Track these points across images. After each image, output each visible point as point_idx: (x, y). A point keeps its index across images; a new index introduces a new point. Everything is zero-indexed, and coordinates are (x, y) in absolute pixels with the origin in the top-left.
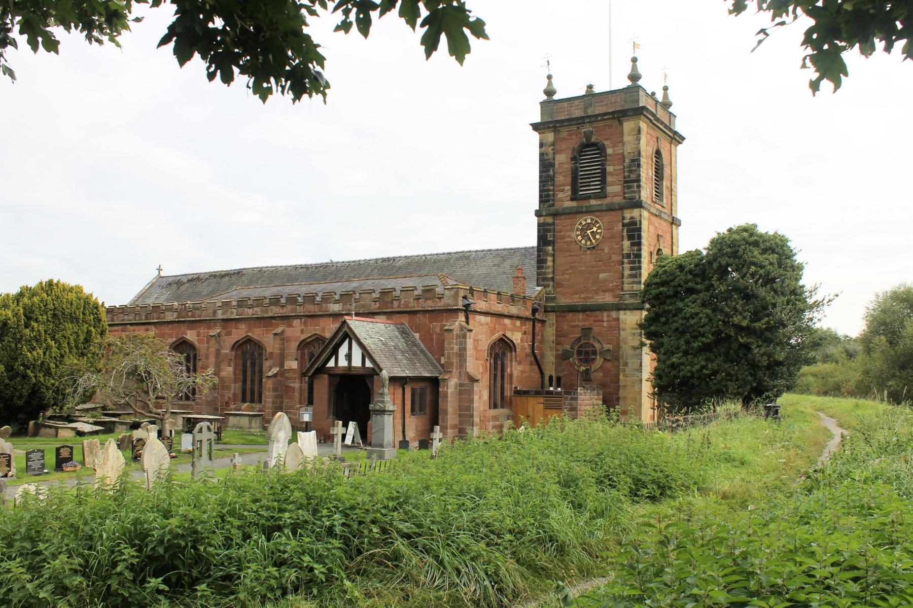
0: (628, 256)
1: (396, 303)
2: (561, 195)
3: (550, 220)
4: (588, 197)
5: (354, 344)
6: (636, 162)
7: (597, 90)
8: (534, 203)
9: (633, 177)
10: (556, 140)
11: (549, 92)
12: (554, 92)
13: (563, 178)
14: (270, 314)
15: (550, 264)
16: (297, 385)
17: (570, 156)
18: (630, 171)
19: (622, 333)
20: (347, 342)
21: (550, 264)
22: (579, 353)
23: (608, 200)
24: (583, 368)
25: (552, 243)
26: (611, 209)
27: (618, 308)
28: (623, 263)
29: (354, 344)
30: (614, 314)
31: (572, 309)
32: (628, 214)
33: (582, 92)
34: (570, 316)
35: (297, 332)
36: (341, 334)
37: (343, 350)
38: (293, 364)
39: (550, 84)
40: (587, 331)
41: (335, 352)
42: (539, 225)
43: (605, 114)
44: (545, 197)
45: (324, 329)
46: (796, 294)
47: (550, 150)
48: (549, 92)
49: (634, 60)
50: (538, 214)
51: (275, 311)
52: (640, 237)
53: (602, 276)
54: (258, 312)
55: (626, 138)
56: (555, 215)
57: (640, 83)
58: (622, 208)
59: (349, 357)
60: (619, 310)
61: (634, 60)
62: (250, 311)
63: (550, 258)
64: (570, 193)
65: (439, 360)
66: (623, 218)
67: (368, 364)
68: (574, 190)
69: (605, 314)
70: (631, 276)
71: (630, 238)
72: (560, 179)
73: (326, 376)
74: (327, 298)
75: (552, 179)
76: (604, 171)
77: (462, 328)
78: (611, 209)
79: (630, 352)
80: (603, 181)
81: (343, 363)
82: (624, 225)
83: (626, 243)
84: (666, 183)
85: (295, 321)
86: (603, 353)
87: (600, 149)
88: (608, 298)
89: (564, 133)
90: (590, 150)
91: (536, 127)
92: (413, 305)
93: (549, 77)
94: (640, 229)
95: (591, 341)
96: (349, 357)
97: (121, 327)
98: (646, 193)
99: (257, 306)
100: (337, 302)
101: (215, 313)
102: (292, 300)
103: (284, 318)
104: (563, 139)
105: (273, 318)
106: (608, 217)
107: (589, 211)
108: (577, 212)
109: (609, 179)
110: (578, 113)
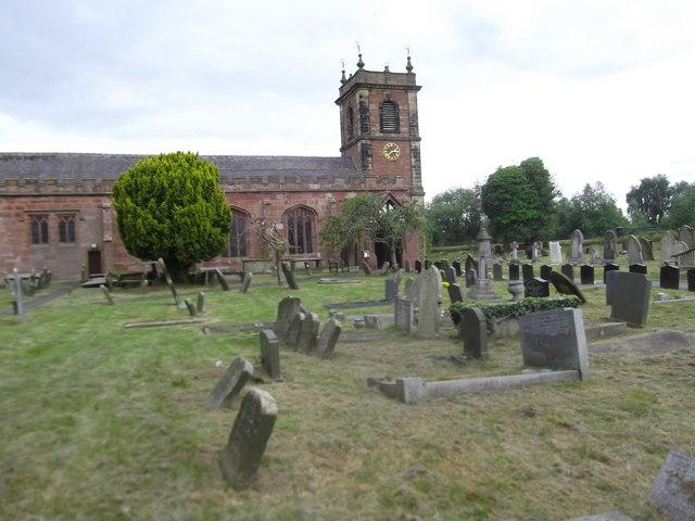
3: (369, 142)
7: (391, 70)
11: (361, 65)
14: (254, 190)
25: (371, 156)
32: (413, 144)
35: (282, 203)
38: (280, 226)
46: (655, 179)
48: (361, 65)
49: (409, 58)
51: (256, 187)
54: (241, 187)
56: (371, 140)
58: (410, 141)
61: (409, 58)
62: (231, 187)
68: (382, 128)
71: (415, 157)
72: (372, 118)
76: (398, 118)
85: (278, 196)
87: (395, 106)
89: (374, 92)
97: (53, 198)
103: (266, 192)
105: (258, 192)
107: (391, 141)
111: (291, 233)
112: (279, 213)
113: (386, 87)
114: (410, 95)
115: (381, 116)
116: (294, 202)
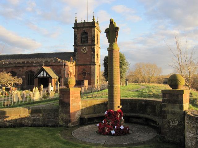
0: (93, 55)
1: (49, 64)
2: (79, 42)
3: (76, 47)
4: (84, 43)
5: (44, 72)
6: (94, 37)
7: (86, 22)
8: (73, 43)
9: (93, 39)
10: (78, 31)
11: (76, 21)
12: (77, 21)
13: (79, 39)
15: (76, 56)
16: (25, 81)
17: (81, 34)
18: (93, 38)
19: (91, 70)
20: (42, 72)
21: (76, 56)
22: (83, 74)
23: (88, 44)
24: (83, 77)
26: (89, 45)
27: (91, 65)
28: (91, 56)
29: (44, 72)
30: (90, 66)
31: (81, 65)
32: (92, 47)
33: (83, 22)
34: (81, 66)
36: (41, 70)
37: (42, 73)
38: (24, 77)
39: (76, 19)
40: (84, 69)
41: (40, 74)
42: (74, 48)
43: (88, 27)
44: (75, 42)
45: (32, 69)
47: (76, 33)
48: (76, 21)
50: (74, 46)
51: (19, 65)
52: (95, 51)
53: (87, 59)
55: (92, 32)
56: (77, 46)
57: (95, 21)
58: (91, 45)
59: (43, 75)
60: (91, 65)
63: (76, 55)
64: (80, 42)
65: (59, 75)
66: (92, 47)
67: (48, 76)
68: (81, 41)
69: (88, 66)
70: (93, 59)
71: (93, 51)
72: (78, 39)
73: (38, 79)
74: (32, 63)
75: (77, 39)
76: (88, 38)
77: (64, 69)
78: (89, 45)
79: (93, 73)
80: (87, 40)
81: (41, 76)
82: (92, 49)
83: (92, 52)
84: (98, 40)
86: (87, 74)
87: (87, 33)
88: (88, 63)
89: (79, 30)
90: (85, 33)
91: (73, 28)
92: (53, 64)
93: (76, 18)
94: (95, 50)
95: (85, 71)
96: (43, 75)
98: (96, 43)
99: (14, 64)
100: (35, 63)
101: (2, 66)
102: (23, 63)
104: (79, 31)
105: (19, 67)
106: (89, 47)
107: (85, 46)
108: (82, 46)
109: (89, 40)
110: (82, 26)
111: (28, 79)
112: (24, 72)
113: (83, 28)
114: (92, 29)
115: (81, 38)
116: (29, 69)
